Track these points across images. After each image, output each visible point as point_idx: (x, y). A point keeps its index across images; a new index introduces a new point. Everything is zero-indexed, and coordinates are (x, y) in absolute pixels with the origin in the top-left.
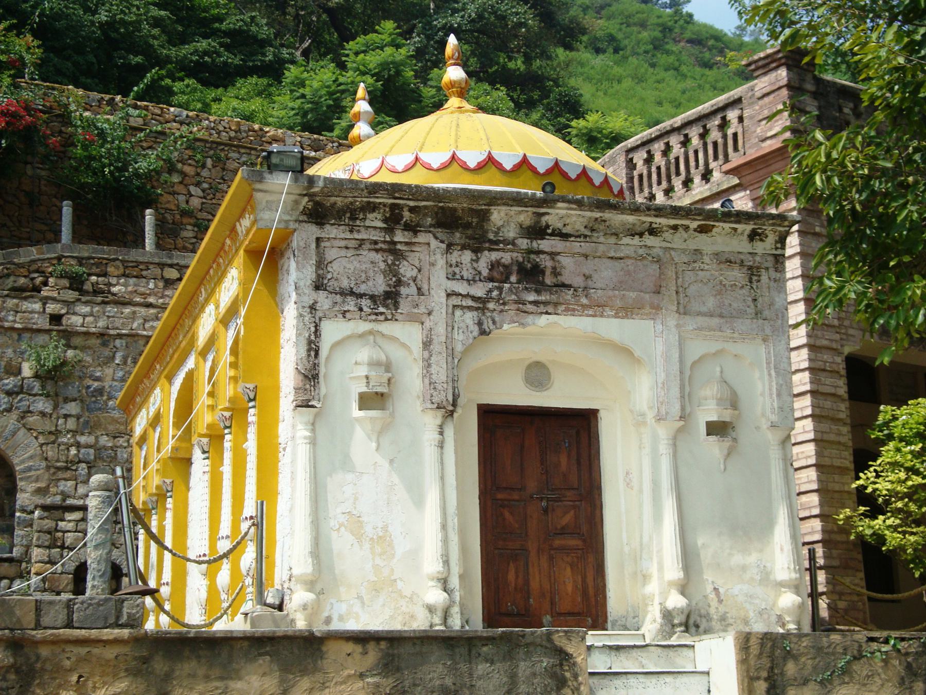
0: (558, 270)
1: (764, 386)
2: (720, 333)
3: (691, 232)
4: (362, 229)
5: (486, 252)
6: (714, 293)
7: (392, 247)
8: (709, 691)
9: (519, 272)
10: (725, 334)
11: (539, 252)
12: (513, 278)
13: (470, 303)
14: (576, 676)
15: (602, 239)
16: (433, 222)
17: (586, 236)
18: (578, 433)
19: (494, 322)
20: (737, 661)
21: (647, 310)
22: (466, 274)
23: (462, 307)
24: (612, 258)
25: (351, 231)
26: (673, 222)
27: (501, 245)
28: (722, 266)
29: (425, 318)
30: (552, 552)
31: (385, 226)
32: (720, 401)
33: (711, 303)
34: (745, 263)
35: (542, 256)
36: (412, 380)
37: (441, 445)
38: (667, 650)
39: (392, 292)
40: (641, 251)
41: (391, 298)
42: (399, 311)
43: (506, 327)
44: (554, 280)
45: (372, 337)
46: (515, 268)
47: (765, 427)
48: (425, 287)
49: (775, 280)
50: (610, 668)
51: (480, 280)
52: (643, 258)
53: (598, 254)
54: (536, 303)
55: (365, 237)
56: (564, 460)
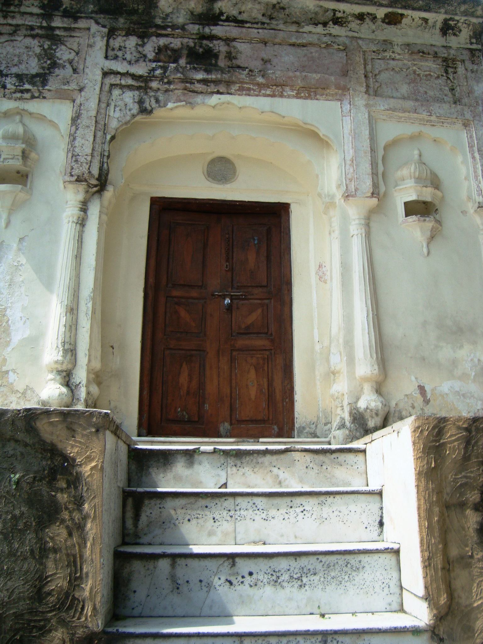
0: (233, 54)
1: (468, 169)
2: (415, 115)
3: (379, 23)
4: (18, 16)
5: (154, 38)
6: (408, 81)
7: (49, 33)
8: (381, 524)
9: (188, 56)
10: (421, 116)
11: (212, 38)
12: (182, 62)
13: (130, 82)
14: (79, 502)
15: (281, 26)
16: (96, 9)
17: (263, 23)
18: (269, 232)
19: (157, 101)
20: (419, 475)
21: (332, 90)
22: (128, 56)
23: (122, 87)
24: (293, 45)
25: (5, 17)
26: (358, 9)
27: (169, 29)
28: (415, 57)
29: (76, 95)
30: (234, 353)
31: (42, 11)
32: (418, 180)
33: (404, 89)
34: (439, 55)
35: (215, 42)
36: (55, 157)
37: (82, 223)
38: (321, 458)
39: (45, 73)
40: (325, 39)
41: (42, 78)
42: (46, 88)
43: (170, 105)
44: (229, 63)
45: (18, 118)
46: (185, 52)
47: (472, 211)
48: (81, 67)
49: (472, 71)
50: (225, 485)
51: (144, 61)
52: (328, 46)
53: (277, 40)
54: (204, 82)
55: (20, 22)
56: (251, 257)
